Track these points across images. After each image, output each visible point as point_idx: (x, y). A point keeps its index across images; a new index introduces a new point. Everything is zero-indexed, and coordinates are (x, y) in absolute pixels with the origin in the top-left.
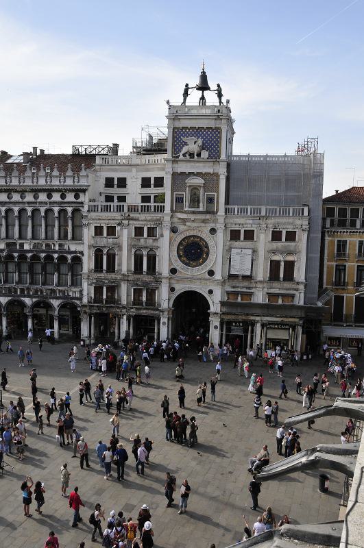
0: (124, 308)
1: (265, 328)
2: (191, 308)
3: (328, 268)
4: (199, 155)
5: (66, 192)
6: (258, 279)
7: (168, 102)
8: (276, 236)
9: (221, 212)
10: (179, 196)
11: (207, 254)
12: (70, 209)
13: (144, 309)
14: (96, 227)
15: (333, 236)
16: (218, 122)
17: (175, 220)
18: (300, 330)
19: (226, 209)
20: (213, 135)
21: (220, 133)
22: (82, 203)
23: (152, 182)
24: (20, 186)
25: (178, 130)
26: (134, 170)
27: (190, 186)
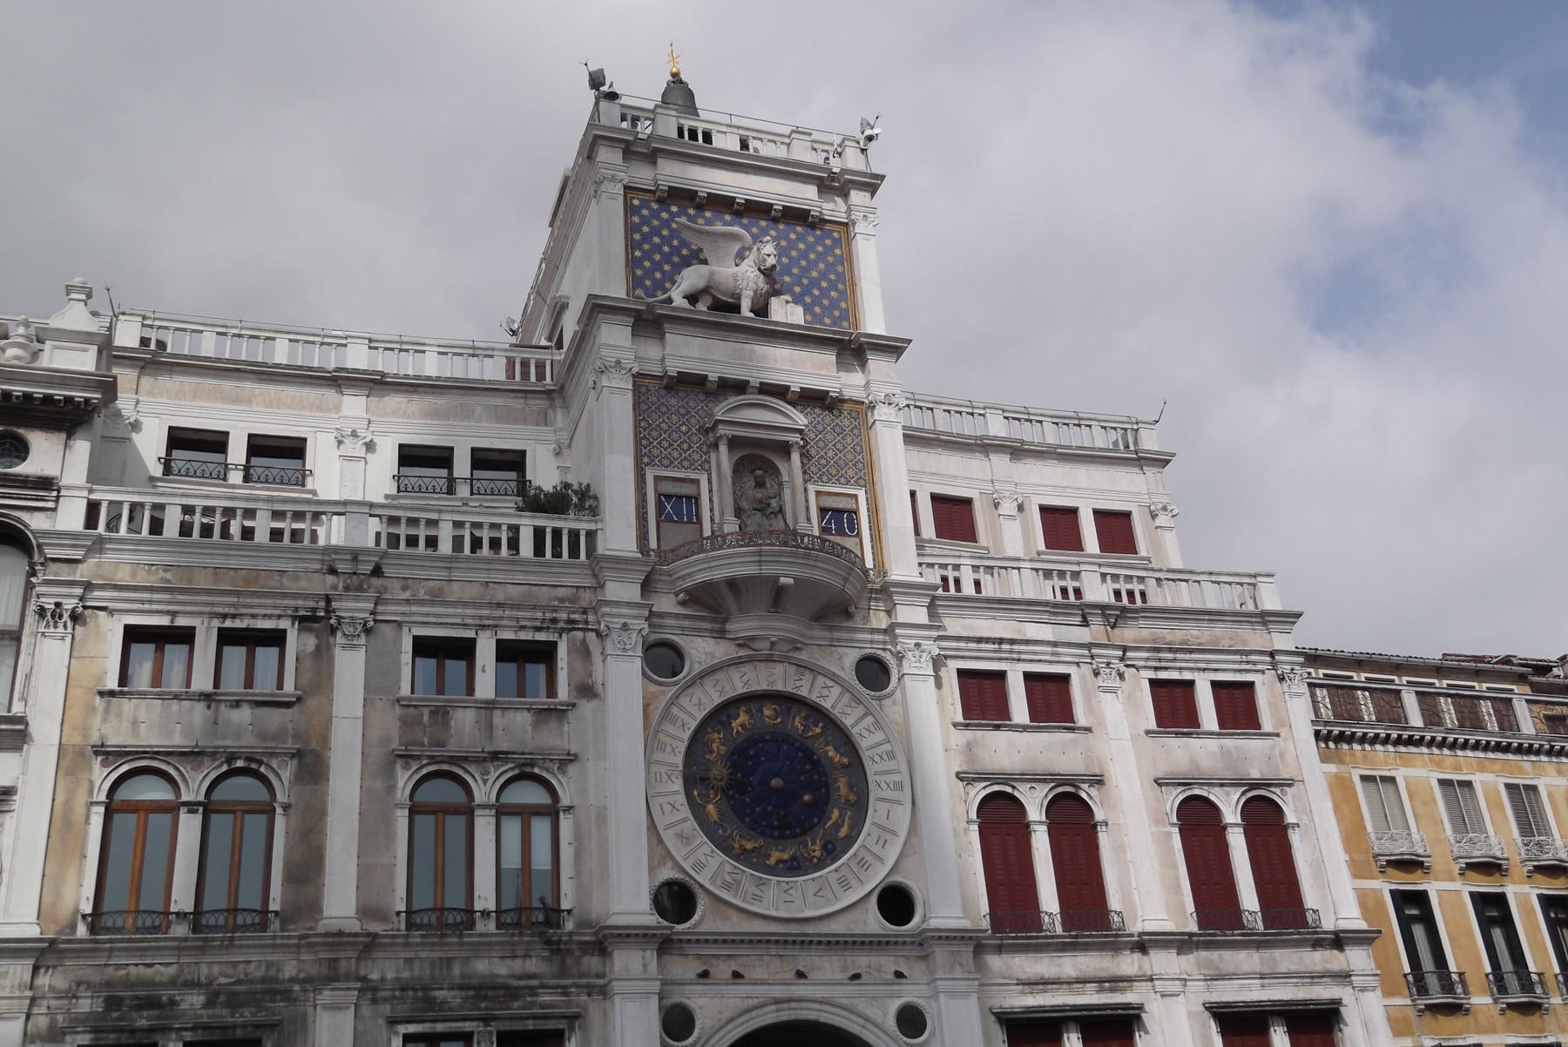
4: (761, 310)
6: (1151, 927)
7: (596, 81)
8: (1174, 707)
14: (133, 635)
15: (1342, 762)
20: (810, 248)
22: (46, 483)
25: (645, 204)
26: (354, 405)
27: (734, 443)
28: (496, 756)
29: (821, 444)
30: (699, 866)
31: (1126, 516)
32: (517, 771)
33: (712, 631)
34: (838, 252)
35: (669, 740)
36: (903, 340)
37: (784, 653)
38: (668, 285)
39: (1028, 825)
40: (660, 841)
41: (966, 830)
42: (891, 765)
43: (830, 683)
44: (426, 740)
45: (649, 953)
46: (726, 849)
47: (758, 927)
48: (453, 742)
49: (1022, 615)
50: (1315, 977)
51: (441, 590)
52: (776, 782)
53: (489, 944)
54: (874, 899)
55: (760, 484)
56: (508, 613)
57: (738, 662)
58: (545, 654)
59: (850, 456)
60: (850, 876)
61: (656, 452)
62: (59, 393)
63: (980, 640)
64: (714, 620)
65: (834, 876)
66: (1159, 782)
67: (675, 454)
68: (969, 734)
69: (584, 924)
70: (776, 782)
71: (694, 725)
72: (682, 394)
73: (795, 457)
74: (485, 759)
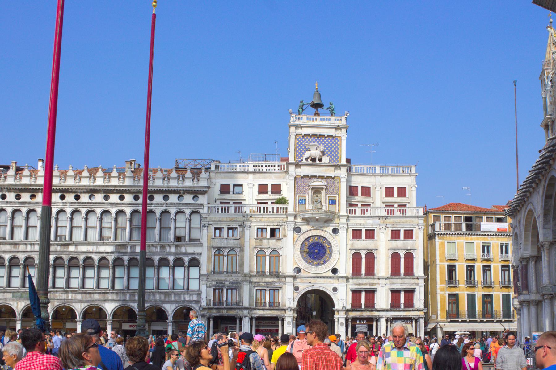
0: (246, 309)
1: (389, 323)
2: (316, 310)
3: (440, 268)
4: (320, 160)
5: (184, 194)
8: (395, 235)
9: (343, 212)
12: (188, 211)
13: (268, 309)
17: (299, 220)
18: (422, 322)
19: (347, 210)
20: (333, 143)
21: (340, 141)
22: (201, 204)
24: (135, 186)
25: (300, 138)
27: (313, 189)
28: (269, 247)
31: (406, 188)
37: (320, 228)
46: (307, 262)
50: (411, 284)
52: (316, 251)
62: (202, 189)
66: (389, 249)
68: (353, 241)
70: (316, 251)
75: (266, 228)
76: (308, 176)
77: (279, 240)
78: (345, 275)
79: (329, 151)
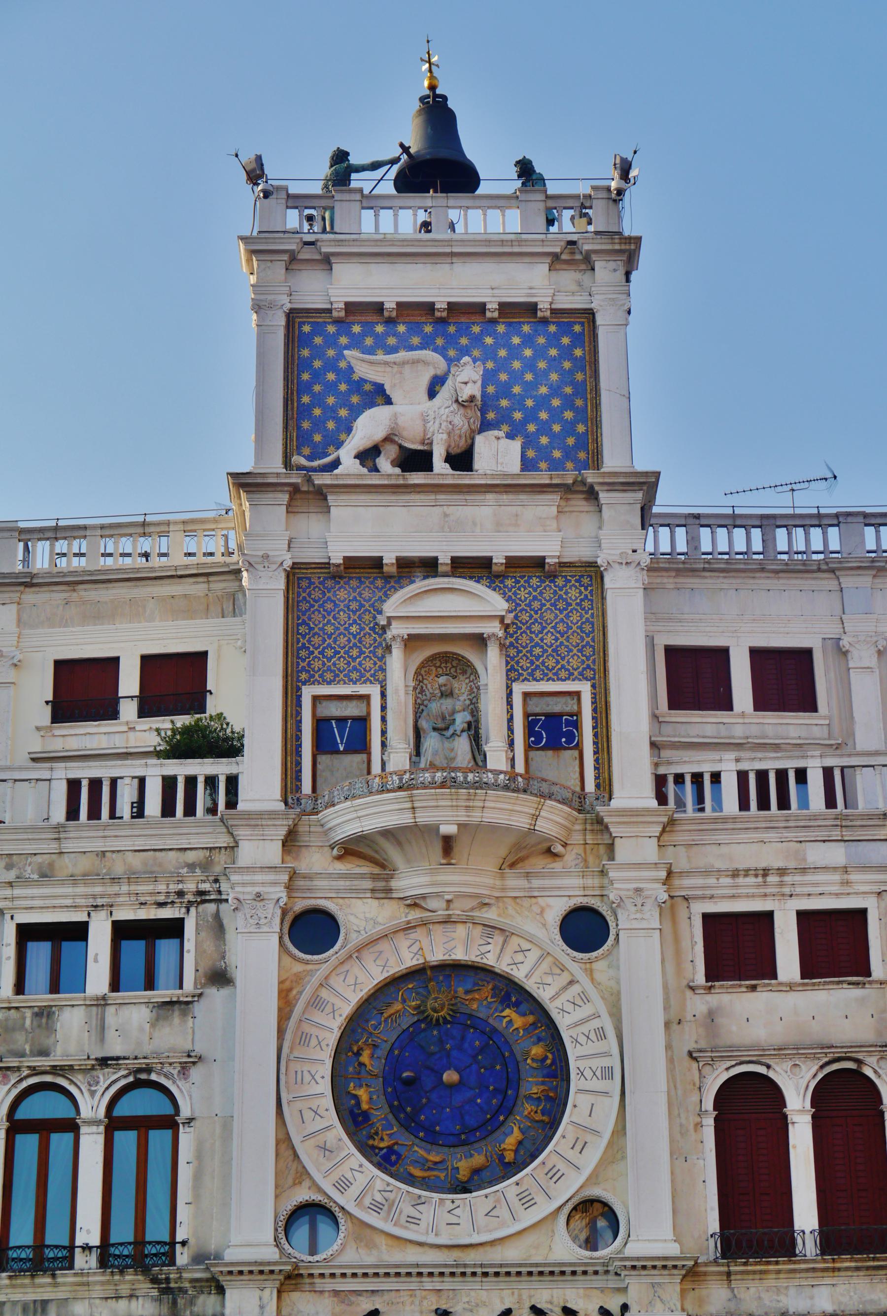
7: (255, 173)
10: (334, 710)
11: (557, 1069)
16: (568, 278)
17: (316, 860)
19: (660, 781)
23: (129, 682)
29: (536, 628)
30: (343, 1185)
32: (131, 1079)
33: (373, 891)
34: (578, 352)
35: (314, 1031)
36: (646, 474)
38: (343, 436)
39: (785, 1117)
40: (296, 1156)
41: (699, 1126)
42: (601, 1046)
43: (526, 945)
44: (27, 1048)
45: (267, 1292)
47: (412, 1256)
48: (59, 1050)
49: (802, 835)
51: (51, 865)
53: (88, 1284)
54: (562, 1218)
55: (447, 694)
56: (125, 888)
57: (408, 928)
58: (175, 929)
59: (575, 640)
60: (535, 1190)
61: (317, 664)
63: (735, 874)
64: (374, 877)
65: (515, 1190)
67: (342, 664)
69: (199, 1258)
70: (450, 1076)
71: (347, 1010)
72: (354, 583)
73: (493, 654)
74: (93, 1068)
75: (78, 932)
76: (376, 563)
77: (182, 1006)
78: (673, 1250)
79: (519, 404)
